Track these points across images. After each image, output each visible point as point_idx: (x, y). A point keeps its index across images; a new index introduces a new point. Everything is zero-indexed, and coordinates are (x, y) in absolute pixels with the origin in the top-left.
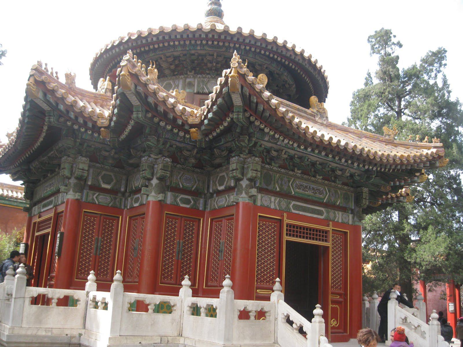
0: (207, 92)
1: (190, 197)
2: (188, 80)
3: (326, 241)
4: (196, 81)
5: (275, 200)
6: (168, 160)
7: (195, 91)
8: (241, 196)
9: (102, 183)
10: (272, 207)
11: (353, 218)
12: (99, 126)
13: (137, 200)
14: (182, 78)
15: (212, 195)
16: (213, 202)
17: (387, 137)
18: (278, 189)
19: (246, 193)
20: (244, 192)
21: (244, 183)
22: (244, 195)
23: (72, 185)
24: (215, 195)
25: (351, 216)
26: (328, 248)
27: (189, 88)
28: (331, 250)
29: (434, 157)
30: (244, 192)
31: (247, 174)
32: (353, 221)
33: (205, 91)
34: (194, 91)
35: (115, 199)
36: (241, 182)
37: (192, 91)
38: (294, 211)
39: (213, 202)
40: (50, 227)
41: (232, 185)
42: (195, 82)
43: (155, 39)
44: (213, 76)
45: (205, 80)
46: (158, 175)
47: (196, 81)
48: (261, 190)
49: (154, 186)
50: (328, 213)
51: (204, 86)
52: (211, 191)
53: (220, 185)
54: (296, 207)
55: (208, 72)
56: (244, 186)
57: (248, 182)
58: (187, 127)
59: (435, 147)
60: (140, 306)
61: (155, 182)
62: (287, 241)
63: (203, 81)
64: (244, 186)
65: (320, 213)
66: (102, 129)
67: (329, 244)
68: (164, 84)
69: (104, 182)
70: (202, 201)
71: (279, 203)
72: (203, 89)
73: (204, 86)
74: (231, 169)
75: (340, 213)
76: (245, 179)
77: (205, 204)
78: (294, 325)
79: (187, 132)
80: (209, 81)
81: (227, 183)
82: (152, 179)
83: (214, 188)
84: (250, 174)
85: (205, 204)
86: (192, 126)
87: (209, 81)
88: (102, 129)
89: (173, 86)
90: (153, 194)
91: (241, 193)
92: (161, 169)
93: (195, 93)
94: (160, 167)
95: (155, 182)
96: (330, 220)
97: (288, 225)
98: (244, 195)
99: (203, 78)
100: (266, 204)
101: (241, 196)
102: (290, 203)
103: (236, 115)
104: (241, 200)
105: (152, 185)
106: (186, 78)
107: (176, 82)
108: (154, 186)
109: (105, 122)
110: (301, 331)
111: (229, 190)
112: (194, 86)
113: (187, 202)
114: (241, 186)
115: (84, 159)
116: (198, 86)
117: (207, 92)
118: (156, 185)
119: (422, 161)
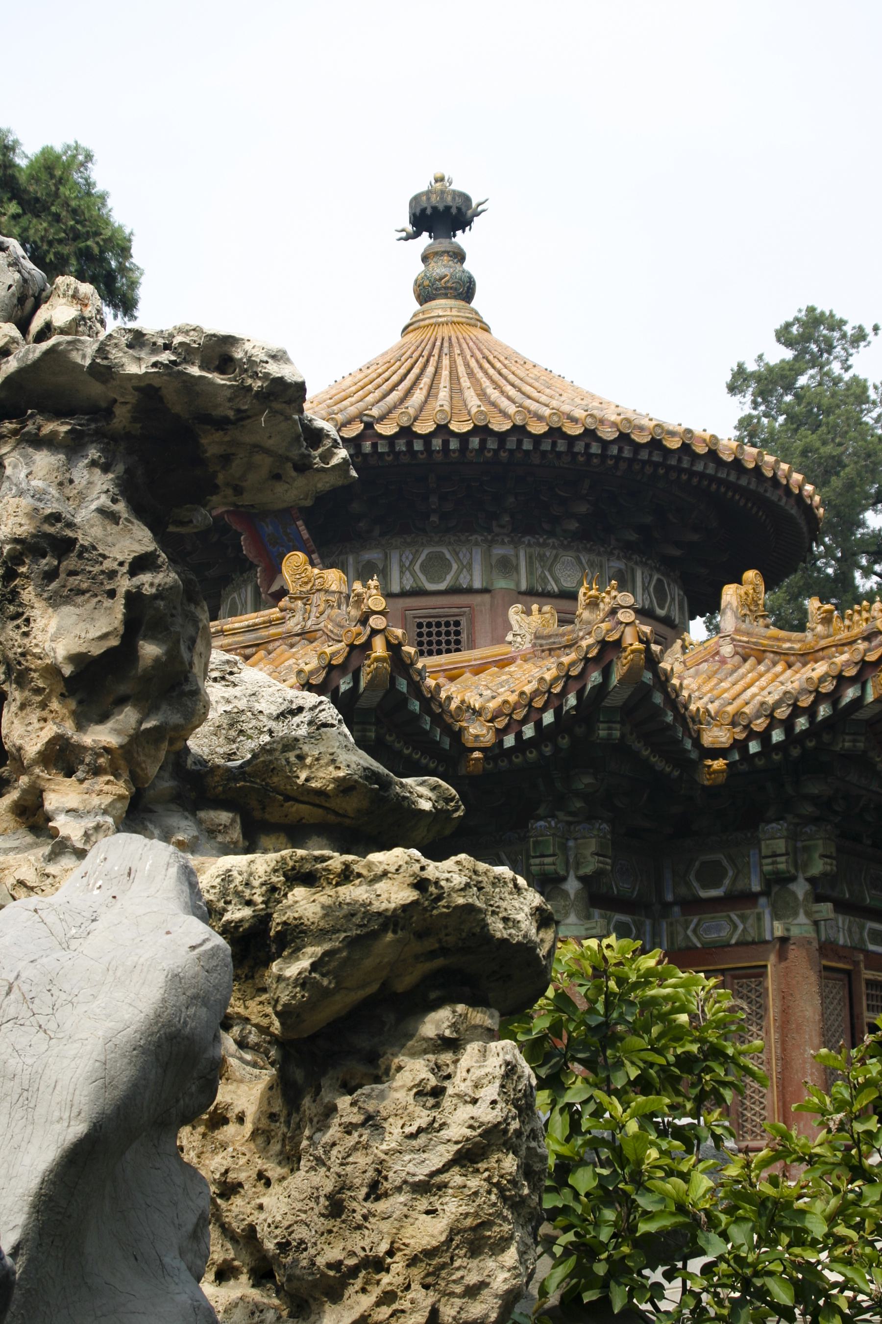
0: (556, 589)
2: (499, 551)
7: (524, 586)
8: (795, 922)
10: (841, 942)
14: (477, 544)
15: (667, 906)
16: (680, 929)
18: (847, 896)
19: (808, 914)
20: (801, 911)
21: (800, 889)
22: (802, 919)
27: (505, 578)
30: (801, 911)
31: (806, 866)
33: (549, 588)
34: (518, 584)
36: (793, 887)
37: (512, 586)
38: (872, 947)
39: (680, 929)
41: (756, 888)
42: (517, 556)
44: (566, 542)
45: (548, 554)
46: (588, 870)
48: (841, 907)
49: (572, 897)
51: (547, 573)
55: (546, 526)
56: (801, 896)
58: (694, 755)
63: (542, 557)
64: (801, 896)
68: (423, 557)
72: (544, 579)
73: (547, 573)
76: (801, 880)
80: (556, 556)
82: (564, 879)
83: (683, 891)
84: (818, 867)
86: (716, 753)
87: (556, 556)
88: (477, 755)
89: (455, 566)
91: (796, 914)
93: (520, 593)
94: (593, 849)
97: (870, 983)
101: (795, 922)
102: (862, 928)
103: (849, 741)
104: (795, 932)
105: (566, 894)
106: (491, 543)
107: (461, 555)
108: (572, 897)
109: (484, 736)
111: (741, 899)
112: (517, 569)
114: (794, 894)
116: (530, 572)
117: (556, 589)
118: (576, 894)
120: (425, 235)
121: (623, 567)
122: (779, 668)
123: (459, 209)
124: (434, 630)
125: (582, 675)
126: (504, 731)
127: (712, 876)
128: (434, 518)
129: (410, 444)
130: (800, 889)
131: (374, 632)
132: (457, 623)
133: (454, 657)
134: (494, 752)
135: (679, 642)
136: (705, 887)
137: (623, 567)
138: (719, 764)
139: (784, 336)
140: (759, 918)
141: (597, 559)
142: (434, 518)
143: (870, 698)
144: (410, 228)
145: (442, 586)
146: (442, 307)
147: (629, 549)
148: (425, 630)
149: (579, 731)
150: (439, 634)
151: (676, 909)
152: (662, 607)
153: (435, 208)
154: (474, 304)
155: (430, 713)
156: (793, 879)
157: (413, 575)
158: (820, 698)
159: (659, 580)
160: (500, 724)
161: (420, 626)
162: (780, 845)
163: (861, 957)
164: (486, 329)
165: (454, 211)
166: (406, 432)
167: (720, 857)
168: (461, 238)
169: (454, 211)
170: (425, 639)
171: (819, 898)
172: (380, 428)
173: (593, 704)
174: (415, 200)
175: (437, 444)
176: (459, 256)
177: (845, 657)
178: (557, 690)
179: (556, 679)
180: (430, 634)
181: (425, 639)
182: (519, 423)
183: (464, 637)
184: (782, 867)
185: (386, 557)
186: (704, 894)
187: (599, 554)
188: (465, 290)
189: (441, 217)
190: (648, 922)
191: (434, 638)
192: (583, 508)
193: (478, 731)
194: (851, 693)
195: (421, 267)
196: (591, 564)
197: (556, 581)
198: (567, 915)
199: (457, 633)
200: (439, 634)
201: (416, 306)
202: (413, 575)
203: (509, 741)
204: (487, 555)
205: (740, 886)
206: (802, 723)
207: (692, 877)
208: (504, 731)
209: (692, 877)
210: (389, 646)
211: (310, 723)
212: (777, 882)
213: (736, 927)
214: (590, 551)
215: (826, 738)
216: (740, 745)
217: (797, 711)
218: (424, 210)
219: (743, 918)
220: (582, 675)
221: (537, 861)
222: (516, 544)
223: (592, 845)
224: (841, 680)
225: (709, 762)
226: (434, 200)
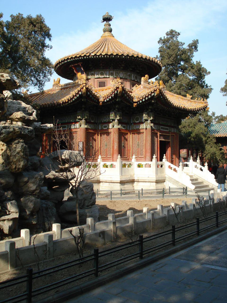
1: (125, 125)
2: (111, 72)
4: (114, 72)
6: (121, 112)
14: (108, 71)
15: (131, 124)
17: (188, 98)
19: (150, 125)
22: (149, 126)
25: (176, 129)
29: (205, 107)
35: (95, 126)
38: (161, 130)
47: (114, 72)
54: (162, 128)
57: (150, 121)
58: (132, 103)
60: (124, 166)
61: (116, 121)
63: (117, 73)
65: (167, 129)
67: (170, 140)
70: (129, 126)
71: (157, 127)
75: (173, 129)
78: (172, 169)
79: (133, 104)
81: (140, 120)
83: (134, 122)
85: (130, 127)
86: (135, 102)
88: (101, 103)
90: (116, 125)
91: (148, 125)
95: (116, 121)
104: (148, 128)
106: (110, 71)
110: (175, 170)
112: (113, 74)
119: (201, 109)
120: (105, 21)
122: (146, 90)
123: (110, 18)
124: (101, 83)
125: (114, 91)
126: (105, 99)
127: (137, 119)
128: (101, 67)
129: (96, 57)
130: (149, 121)
131: (84, 86)
132: (105, 82)
133: (103, 88)
134: (103, 102)
136: (136, 121)
138: (136, 104)
141: (126, 73)
142: (101, 67)
143: (155, 95)
144: (103, 20)
145: (103, 77)
146: (107, 34)
147: (131, 71)
148: (100, 83)
149: (115, 99)
150: (102, 84)
151: (133, 124)
152: (136, 80)
153: (106, 18)
154: (112, 33)
155: (94, 97)
156: (148, 120)
158: (149, 95)
159: (136, 76)
160: (104, 98)
161: (99, 83)
164: (114, 37)
165: (109, 18)
166: (95, 55)
167: (138, 117)
168: (110, 22)
169: (109, 18)
170: (100, 85)
171: (152, 123)
172: (92, 54)
173: (116, 95)
174: (103, 16)
176: (110, 25)
177: (152, 89)
178: (111, 94)
179: (111, 92)
180: (101, 84)
181: (100, 85)
182: (112, 53)
183: (106, 84)
184: (146, 118)
185: (95, 73)
186: (136, 122)
188: (111, 31)
190: (129, 126)
191: (101, 85)
192: (123, 65)
193: (101, 100)
194: (153, 94)
195: (104, 27)
196: (125, 73)
199: (105, 84)
200: (102, 84)
201: (103, 33)
203: (105, 101)
204: (109, 72)
205: (141, 121)
206: (147, 98)
208: (105, 99)
210: (86, 88)
211: (28, 109)
214: (124, 71)
215: (151, 101)
216: (139, 101)
217: (146, 97)
218: (104, 18)
220: (114, 91)
224: (152, 92)
225: (134, 104)
226: (106, 16)
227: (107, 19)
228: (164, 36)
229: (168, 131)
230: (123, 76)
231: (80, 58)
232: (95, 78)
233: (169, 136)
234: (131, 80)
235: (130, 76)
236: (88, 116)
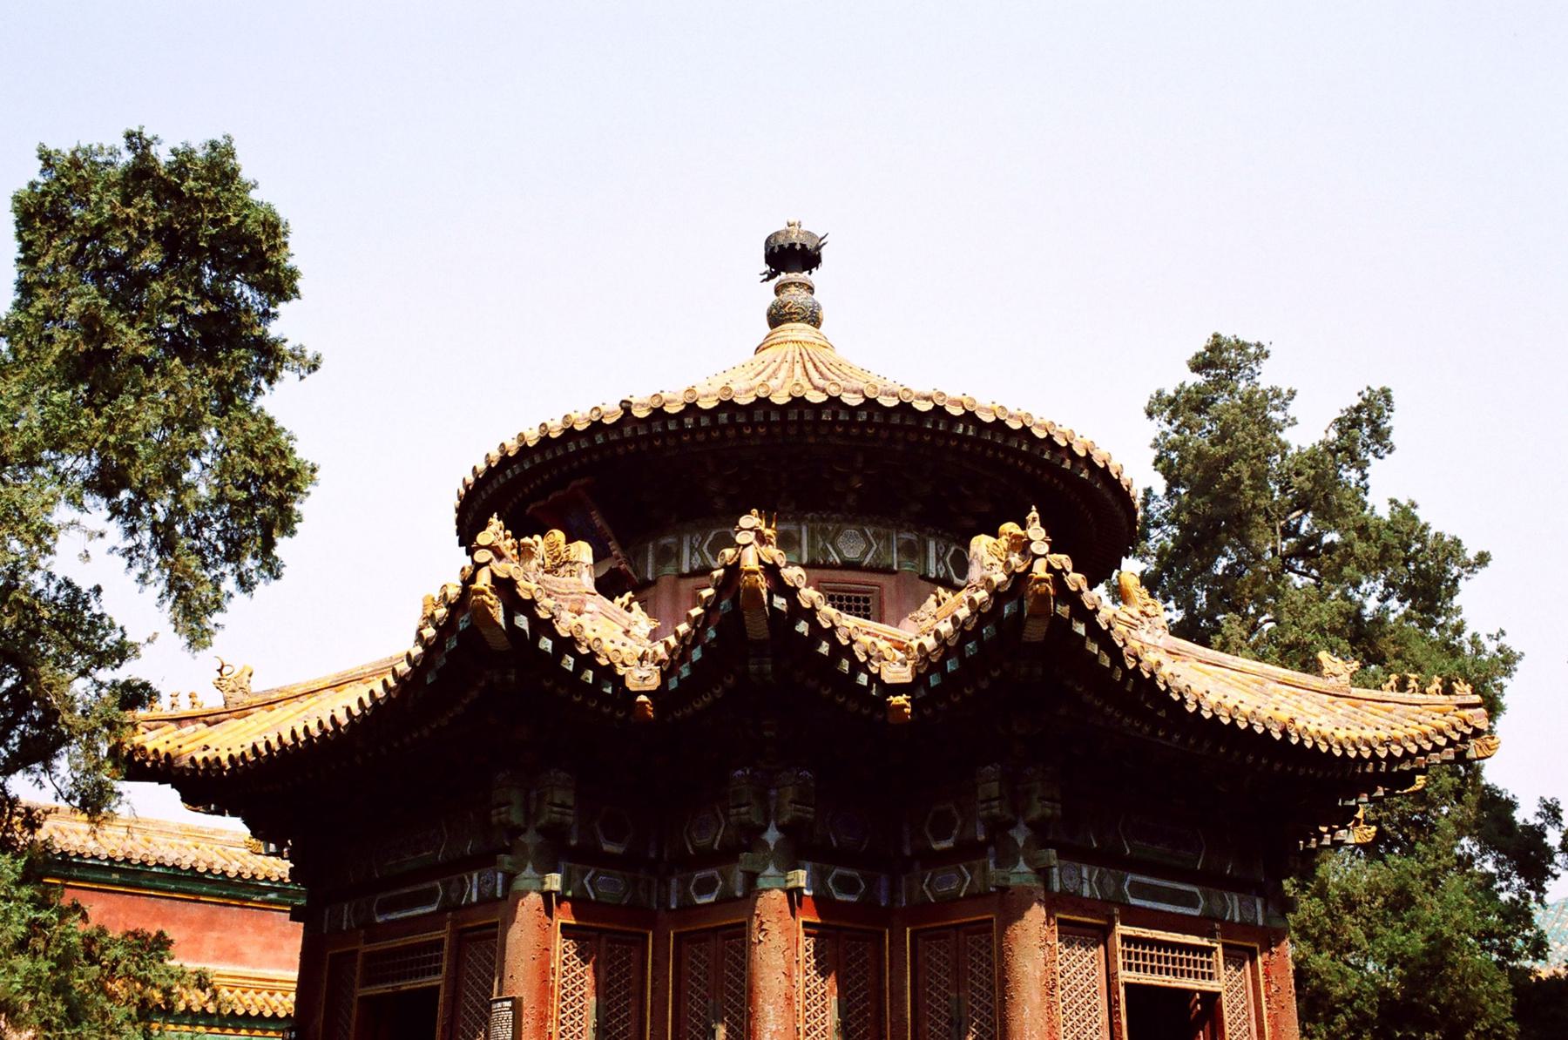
3: (1211, 976)
4: (804, 529)
5: (1090, 875)
9: (602, 839)
10: (1086, 892)
11: (1265, 907)
12: (632, 689)
13: (706, 886)
19: (1027, 862)
22: (1022, 866)
23: (531, 849)
24: (917, 865)
26: (1212, 999)
28: (1224, 998)
32: (1266, 918)
34: (800, 557)
38: (1134, 901)
40: (437, 971)
42: (800, 532)
43: (704, 422)
46: (785, 819)
47: (804, 529)
50: (1207, 899)
52: (908, 852)
53: (938, 839)
54: (1139, 890)
56: (1021, 842)
59: (1462, 706)
61: (772, 836)
62: (1128, 986)
63: (824, 532)
64: (1021, 842)
65: (1190, 901)
66: (643, 698)
69: (610, 839)
70: (884, 882)
71: (1100, 882)
72: (826, 552)
74: (981, 797)
77: (894, 890)
82: (765, 829)
84: (1037, 811)
85: (894, 890)
86: (898, 689)
91: (1016, 863)
92: (791, 802)
96: (1217, 920)
97: (1127, 939)
98: (1022, 866)
99: (823, 520)
100: (1071, 886)
102: (1123, 880)
111: (968, 851)
112: (800, 546)
113: (847, 885)
115: (562, 775)
116: (812, 545)
121: (914, 538)
130: (1020, 836)
135: (933, 597)
137: (914, 538)
139: (1198, 365)
140: (985, 868)
141: (883, 531)
153: (781, 247)
154: (821, 329)
157: (702, 555)
162: (994, 788)
163: (1116, 911)
175: (689, 422)
182: (762, 395)
184: (996, 811)
185: (680, 542)
187: (887, 527)
189: (790, 257)
195: (774, 298)
196: (877, 536)
197: (839, 553)
198: (766, 867)
202: (702, 555)
207: (926, 830)
209: (926, 830)
212: (1000, 829)
213: (964, 879)
214: (877, 524)
219: (971, 870)
221: (734, 811)
222: (799, 521)
223: (790, 793)
227: (790, 257)
228: (1179, 377)
229: (1196, 913)
230: (865, 554)
231: (572, 447)
232: (682, 576)
233: (1209, 951)
234: (925, 577)
235: (910, 550)
236: (570, 802)
